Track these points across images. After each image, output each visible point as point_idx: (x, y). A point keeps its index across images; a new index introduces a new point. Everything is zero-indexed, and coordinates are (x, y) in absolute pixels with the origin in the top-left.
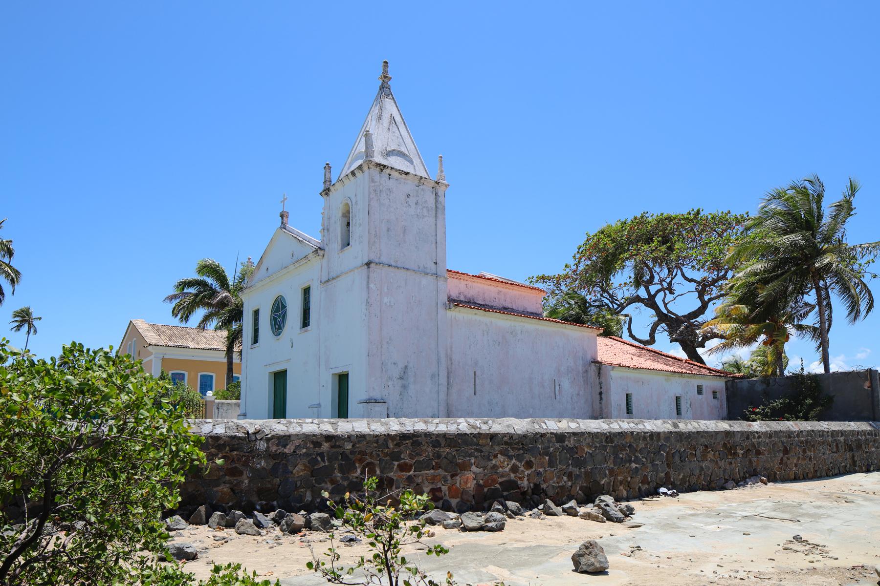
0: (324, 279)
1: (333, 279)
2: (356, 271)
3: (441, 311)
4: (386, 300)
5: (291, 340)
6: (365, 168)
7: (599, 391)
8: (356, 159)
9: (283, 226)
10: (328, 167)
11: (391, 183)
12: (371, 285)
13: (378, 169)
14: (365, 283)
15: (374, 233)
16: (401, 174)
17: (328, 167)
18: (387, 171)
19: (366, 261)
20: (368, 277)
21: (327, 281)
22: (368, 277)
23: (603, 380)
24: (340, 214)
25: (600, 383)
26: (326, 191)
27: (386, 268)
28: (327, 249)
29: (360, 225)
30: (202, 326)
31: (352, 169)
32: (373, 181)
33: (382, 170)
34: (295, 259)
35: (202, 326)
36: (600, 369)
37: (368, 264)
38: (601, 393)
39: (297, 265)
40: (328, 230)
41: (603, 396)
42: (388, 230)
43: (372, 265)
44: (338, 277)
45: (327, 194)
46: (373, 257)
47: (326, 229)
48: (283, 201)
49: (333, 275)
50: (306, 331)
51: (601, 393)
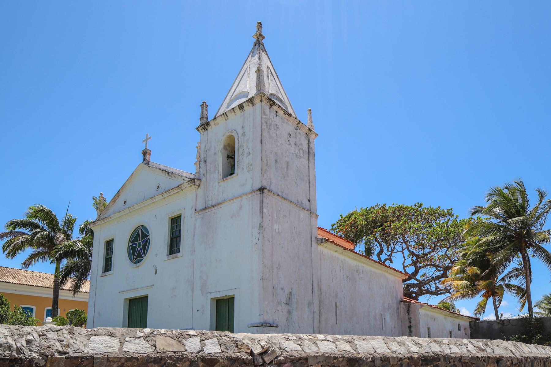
0: (200, 206)
1: (213, 206)
2: (244, 197)
3: (314, 244)
4: (276, 227)
5: (155, 267)
6: (257, 101)
7: (408, 324)
8: (237, 98)
9: (146, 162)
10: (204, 105)
11: (277, 120)
12: (265, 210)
13: (268, 103)
14: (258, 208)
15: (265, 162)
16: (285, 114)
17: (204, 105)
18: (275, 108)
19: (259, 187)
20: (262, 202)
21: (205, 209)
22: (262, 202)
23: (412, 316)
24: (222, 146)
25: (410, 319)
26: (205, 126)
27: (275, 197)
28: (204, 179)
29: (249, 154)
30: (27, 264)
31: (233, 106)
32: (264, 113)
33: (271, 106)
34: (161, 189)
35: (27, 264)
36: (409, 307)
37: (262, 190)
38: (410, 327)
39: (165, 195)
40: (205, 162)
41: (412, 329)
42: (276, 162)
43: (265, 191)
44: (219, 204)
45: (205, 129)
46: (265, 184)
47: (202, 161)
48: (146, 140)
49: (210, 203)
50: (176, 257)
51: (410, 327)
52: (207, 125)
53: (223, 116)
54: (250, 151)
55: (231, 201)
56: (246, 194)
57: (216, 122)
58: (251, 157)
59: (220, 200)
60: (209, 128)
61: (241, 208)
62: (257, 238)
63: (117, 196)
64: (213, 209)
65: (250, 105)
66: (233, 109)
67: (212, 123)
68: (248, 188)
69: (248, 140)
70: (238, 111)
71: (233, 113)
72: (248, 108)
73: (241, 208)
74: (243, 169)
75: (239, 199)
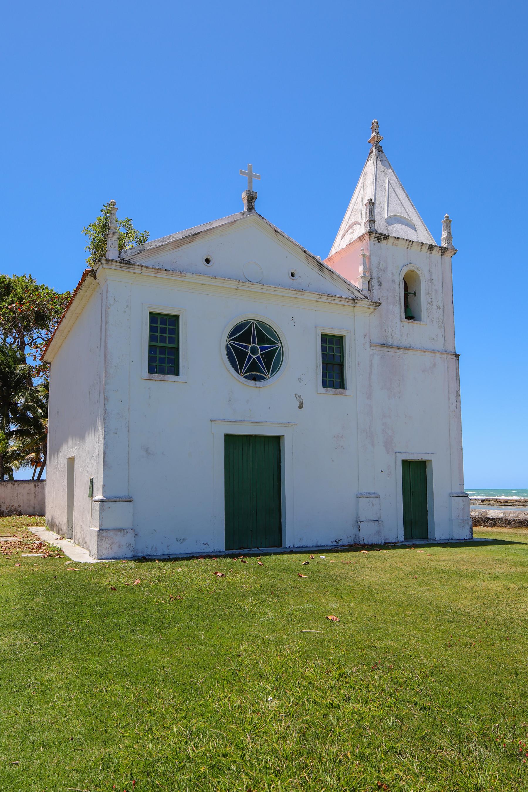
1: (399, 348)
2: (438, 355)
29: (439, 308)
39: (324, 299)
44: (408, 348)
45: (379, 239)
52: (385, 238)
53: (408, 242)
54: (441, 306)
55: (422, 353)
56: (442, 353)
57: (396, 242)
58: (441, 312)
59: (404, 343)
60: (384, 242)
61: (435, 365)
62: (455, 405)
63: (188, 240)
64: (398, 351)
65: (440, 253)
66: (423, 244)
67: (391, 240)
68: (440, 346)
69: (436, 291)
70: (425, 249)
71: (420, 247)
72: (436, 253)
73: (435, 365)
74: (432, 321)
75: (432, 355)
